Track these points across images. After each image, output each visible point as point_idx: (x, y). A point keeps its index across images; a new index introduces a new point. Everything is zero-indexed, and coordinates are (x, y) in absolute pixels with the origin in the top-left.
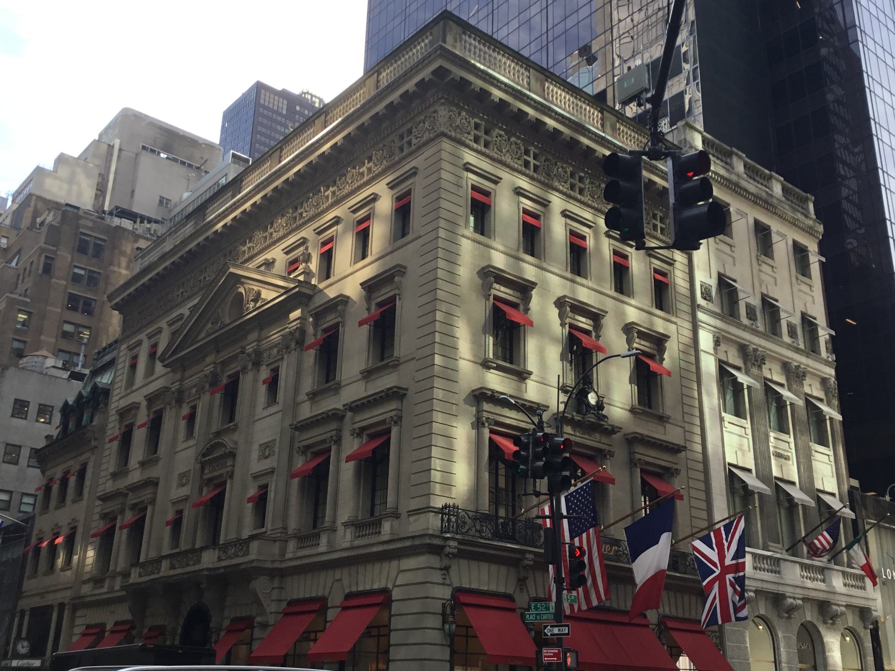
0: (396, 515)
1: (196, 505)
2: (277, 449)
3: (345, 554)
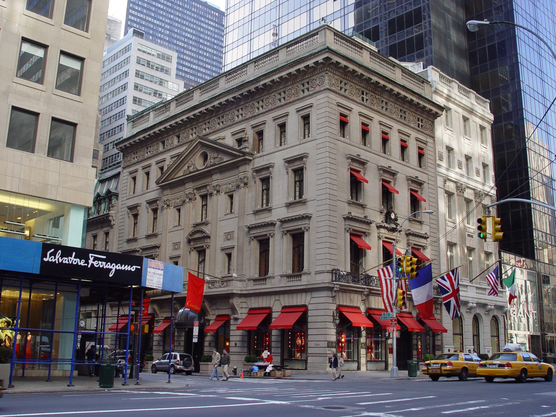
2: (236, 235)
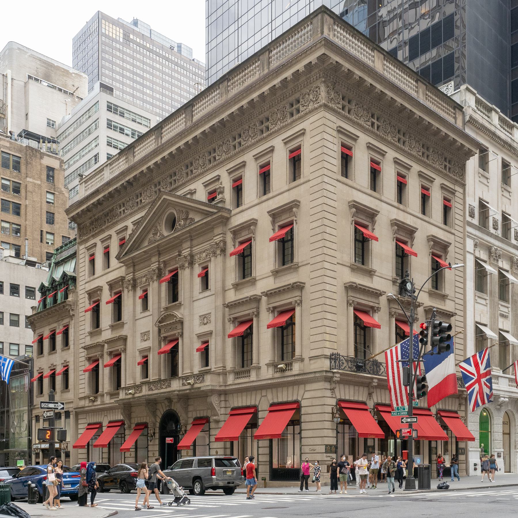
0: (302, 360)
1: (160, 353)
2: (213, 318)
3: (270, 382)
